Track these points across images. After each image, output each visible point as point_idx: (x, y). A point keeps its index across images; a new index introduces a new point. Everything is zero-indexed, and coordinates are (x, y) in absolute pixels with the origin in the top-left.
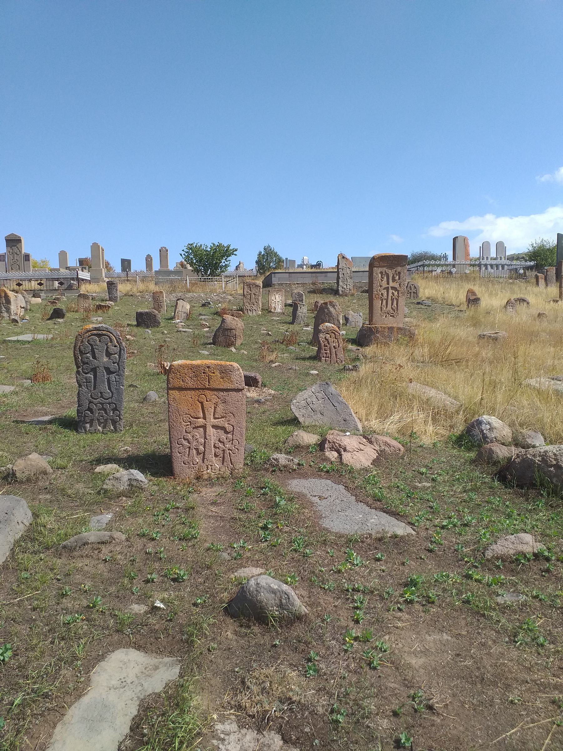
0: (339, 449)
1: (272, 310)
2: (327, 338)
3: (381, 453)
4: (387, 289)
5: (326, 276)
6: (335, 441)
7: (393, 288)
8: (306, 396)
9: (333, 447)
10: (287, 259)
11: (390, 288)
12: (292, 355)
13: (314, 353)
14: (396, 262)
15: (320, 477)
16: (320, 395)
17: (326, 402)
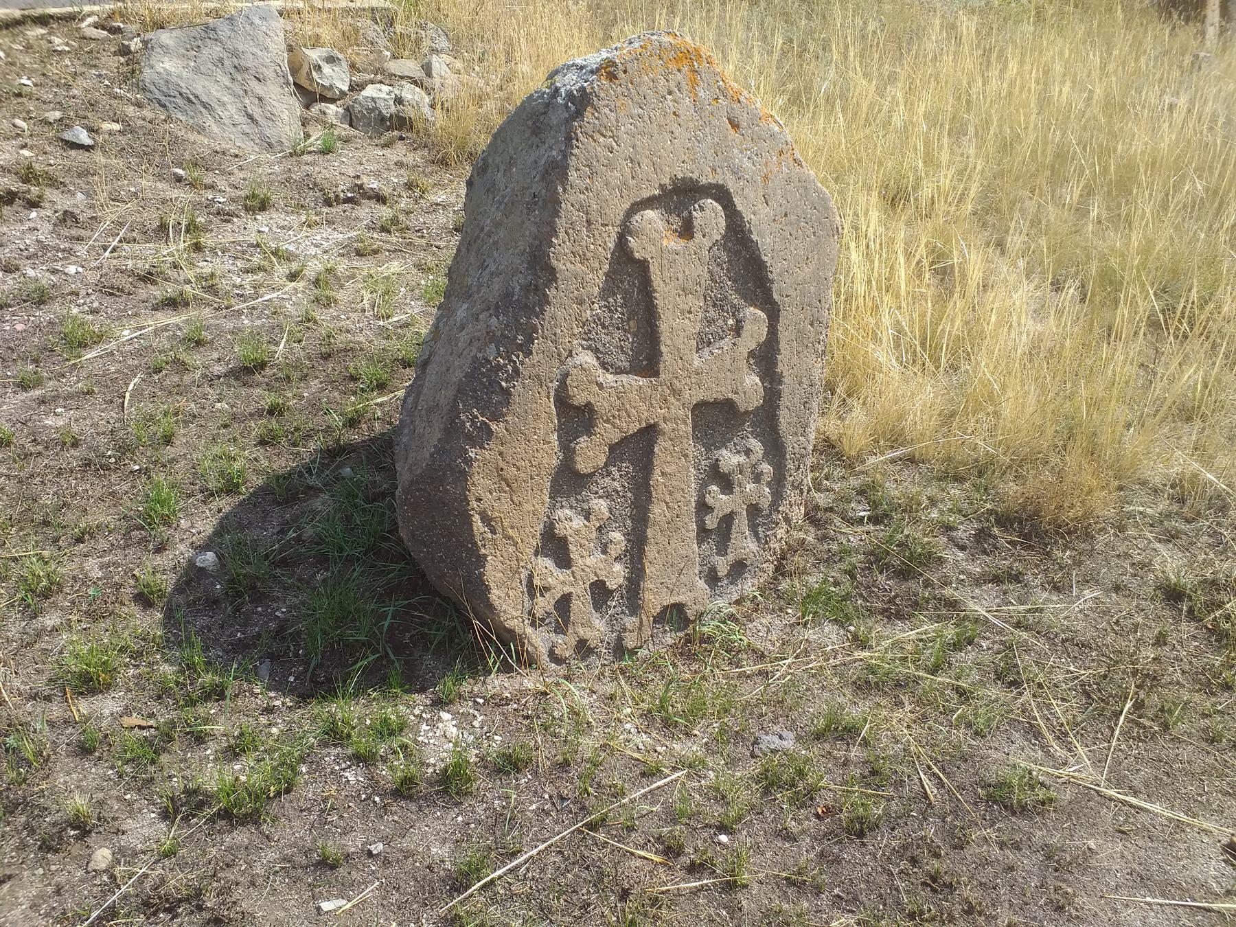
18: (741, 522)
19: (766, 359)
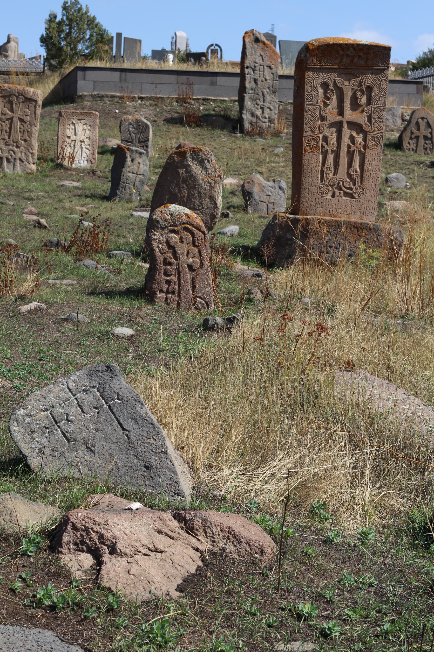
0: (99, 548)
1: (66, 163)
2: (172, 242)
3: (213, 561)
4: (338, 126)
5: (213, 84)
6: (90, 525)
7: (352, 125)
8: (51, 399)
9: (83, 542)
10: (119, 35)
11: (345, 125)
12: (85, 283)
13: (138, 281)
14: (362, 62)
15: (31, 621)
16: (88, 399)
17: (102, 417)
18: (429, 149)
19: (431, 133)
